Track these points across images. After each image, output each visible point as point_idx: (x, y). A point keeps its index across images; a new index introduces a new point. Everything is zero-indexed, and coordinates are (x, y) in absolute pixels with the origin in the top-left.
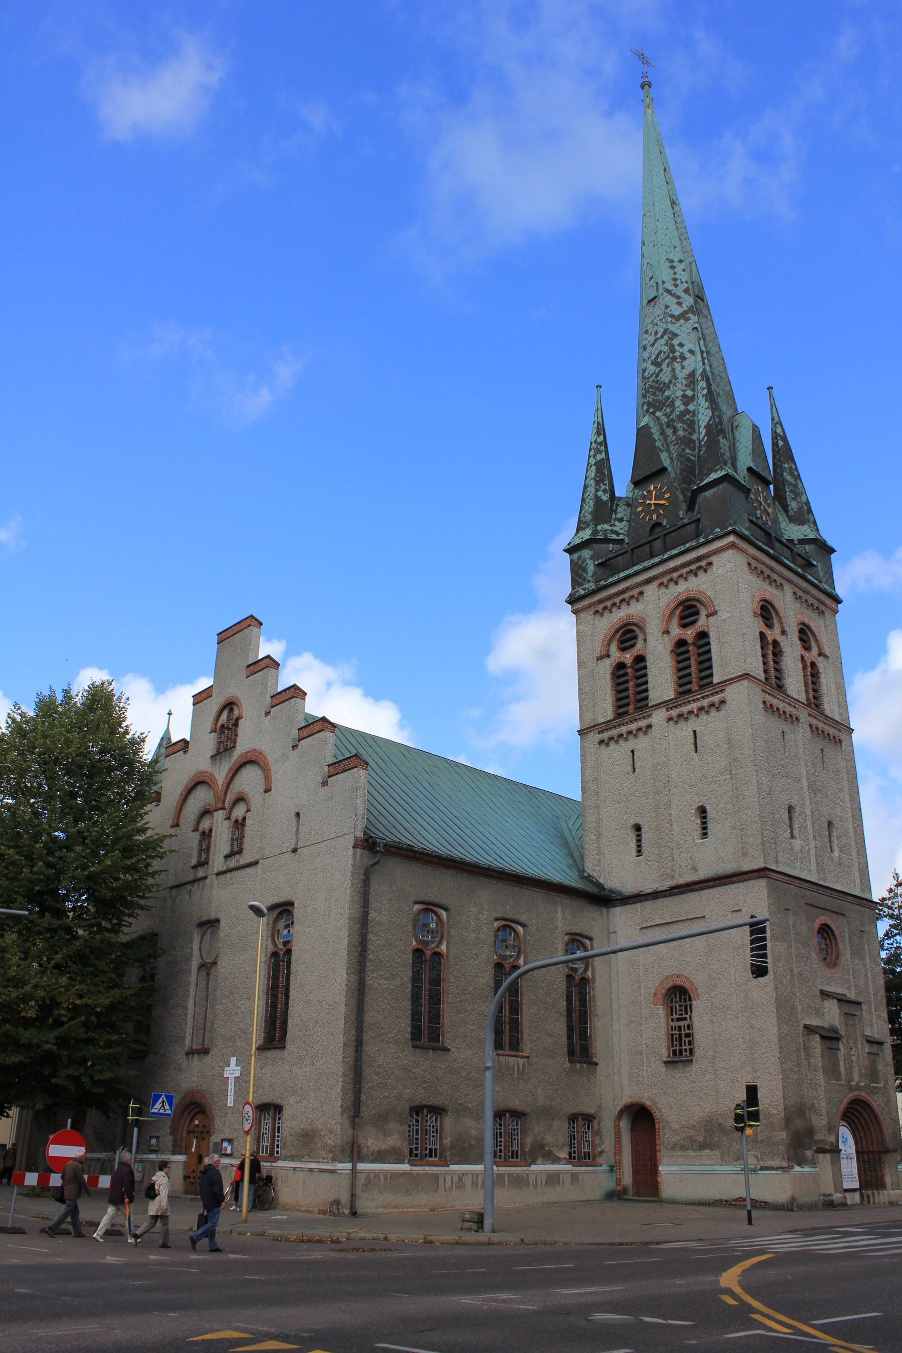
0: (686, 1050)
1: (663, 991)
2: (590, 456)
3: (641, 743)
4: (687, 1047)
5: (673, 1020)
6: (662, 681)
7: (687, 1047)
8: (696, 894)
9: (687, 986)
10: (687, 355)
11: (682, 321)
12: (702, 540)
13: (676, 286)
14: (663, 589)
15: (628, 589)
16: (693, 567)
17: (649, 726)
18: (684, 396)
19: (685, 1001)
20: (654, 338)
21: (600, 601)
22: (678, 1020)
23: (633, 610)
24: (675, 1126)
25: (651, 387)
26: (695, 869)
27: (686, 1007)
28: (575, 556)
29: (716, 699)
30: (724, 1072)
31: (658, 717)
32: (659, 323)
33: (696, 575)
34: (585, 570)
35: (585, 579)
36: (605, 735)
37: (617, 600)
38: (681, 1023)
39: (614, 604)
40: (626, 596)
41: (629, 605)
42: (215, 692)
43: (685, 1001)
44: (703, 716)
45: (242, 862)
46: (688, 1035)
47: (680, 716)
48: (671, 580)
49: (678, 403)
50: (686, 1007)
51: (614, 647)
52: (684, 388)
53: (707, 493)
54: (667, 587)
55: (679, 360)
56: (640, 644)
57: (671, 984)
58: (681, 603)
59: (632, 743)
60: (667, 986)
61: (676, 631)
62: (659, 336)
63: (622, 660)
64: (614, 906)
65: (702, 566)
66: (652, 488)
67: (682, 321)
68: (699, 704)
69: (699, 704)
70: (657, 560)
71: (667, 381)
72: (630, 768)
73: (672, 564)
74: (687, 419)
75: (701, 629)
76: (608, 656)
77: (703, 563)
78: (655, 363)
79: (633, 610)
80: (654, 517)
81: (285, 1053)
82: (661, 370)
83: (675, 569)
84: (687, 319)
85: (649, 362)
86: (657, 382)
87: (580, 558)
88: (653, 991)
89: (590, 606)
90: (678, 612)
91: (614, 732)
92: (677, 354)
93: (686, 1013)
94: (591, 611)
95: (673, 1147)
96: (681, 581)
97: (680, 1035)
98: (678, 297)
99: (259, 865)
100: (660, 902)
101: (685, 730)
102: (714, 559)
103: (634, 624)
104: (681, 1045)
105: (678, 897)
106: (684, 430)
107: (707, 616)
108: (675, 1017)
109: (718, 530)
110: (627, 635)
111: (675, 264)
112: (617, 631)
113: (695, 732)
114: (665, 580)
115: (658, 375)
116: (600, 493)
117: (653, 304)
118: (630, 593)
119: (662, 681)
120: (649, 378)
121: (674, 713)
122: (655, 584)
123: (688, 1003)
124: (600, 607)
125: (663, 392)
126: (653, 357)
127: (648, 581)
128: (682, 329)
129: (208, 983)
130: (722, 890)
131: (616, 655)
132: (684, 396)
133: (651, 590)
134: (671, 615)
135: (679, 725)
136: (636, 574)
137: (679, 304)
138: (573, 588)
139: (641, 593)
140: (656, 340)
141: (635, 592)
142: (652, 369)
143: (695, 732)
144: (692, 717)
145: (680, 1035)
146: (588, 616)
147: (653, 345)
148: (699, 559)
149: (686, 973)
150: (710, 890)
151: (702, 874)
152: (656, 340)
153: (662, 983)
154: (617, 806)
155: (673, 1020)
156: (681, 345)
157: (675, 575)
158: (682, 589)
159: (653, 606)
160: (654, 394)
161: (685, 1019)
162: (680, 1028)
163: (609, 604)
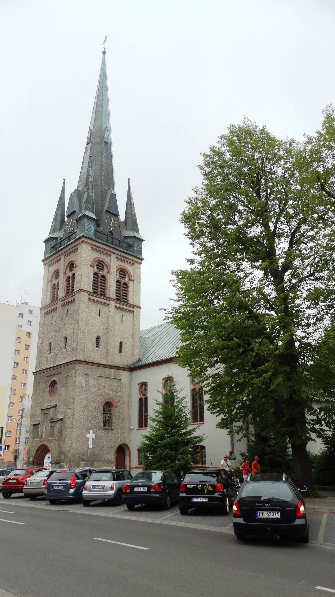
3: (104, 309)
6: (111, 290)
17: (108, 304)
21: (95, 246)
29: (131, 309)
46: (108, 420)
56: (105, 272)
79: (106, 259)
103: (106, 265)
119: (111, 290)
121: (118, 305)
124: (94, 248)
127: (114, 253)
133: (113, 257)
141: (109, 253)
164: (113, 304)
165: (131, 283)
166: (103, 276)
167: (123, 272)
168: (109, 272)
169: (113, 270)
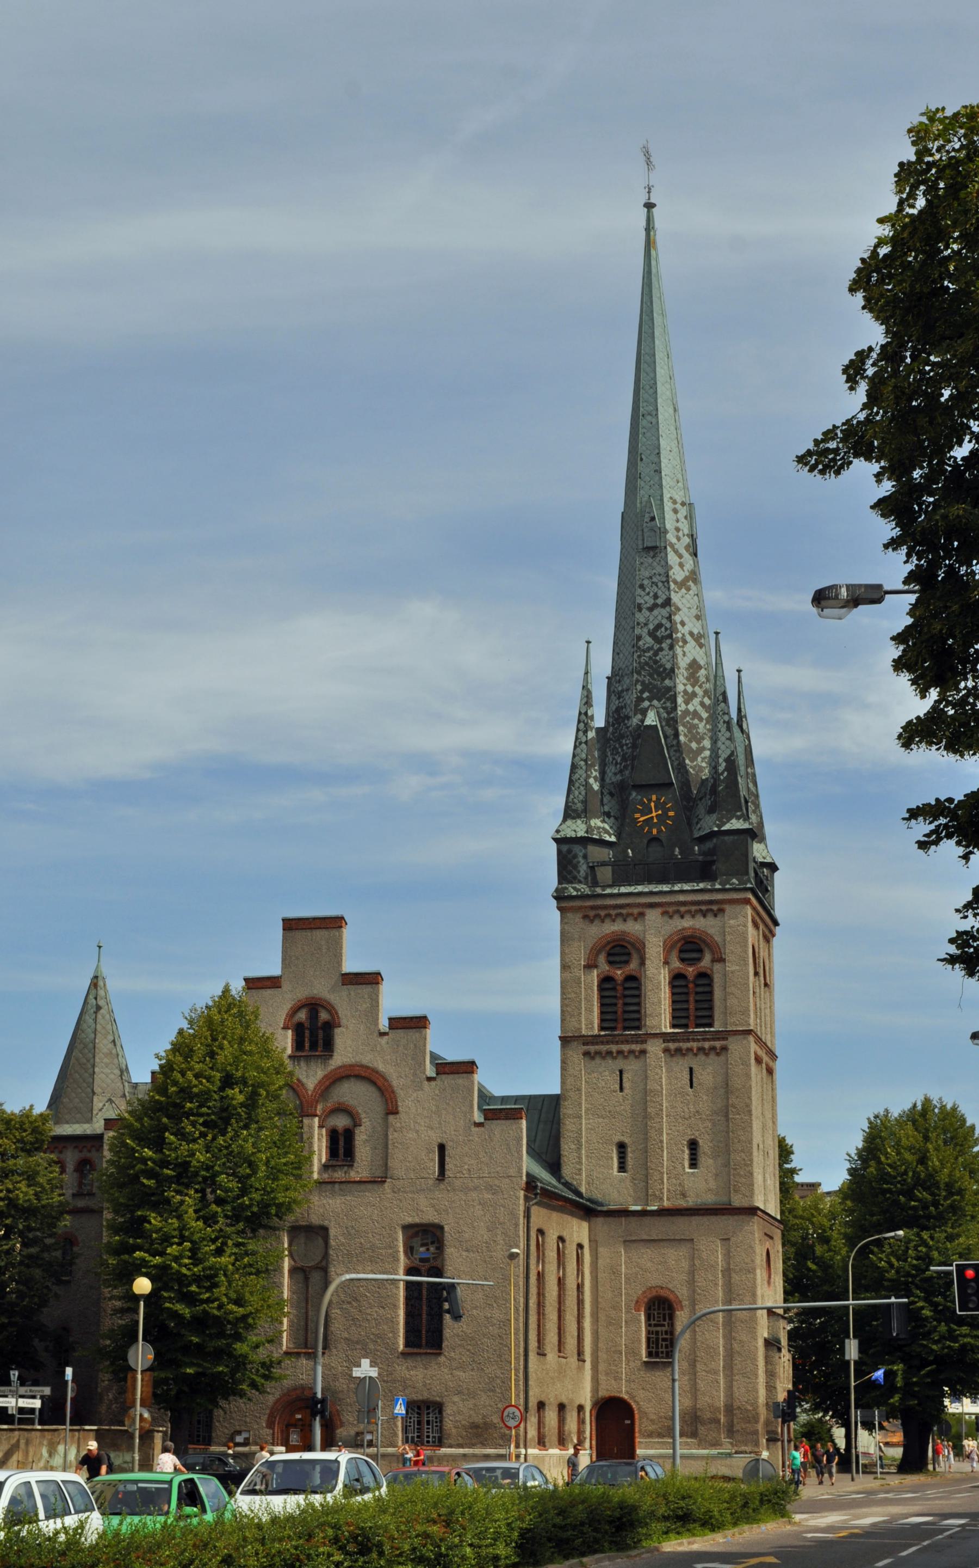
0: (662, 1352)
1: (646, 1300)
2: (578, 730)
3: (632, 1067)
4: (664, 1350)
5: (650, 1325)
7: (664, 1350)
8: (686, 1218)
9: (671, 1297)
10: (688, 638)
11: (683, 591)
12: (718, 886)
13: (679, 539)
14: (666, 918)
15: (628, 905)
16: (704, 908)
18: (685, 692)
19: (664, 1309)
20: (652, 601)
21: (592, 908)
22: (656, 1325)
23: (632, 928)
24: (654, 1417)
25: (646, 664)
26: (684, 1195)
27: (664, 1315)
28: (565, 848)
29: (718, 1044)
30: (704, 1373)
31: (655, 1048)
32: (660, 584)
33: (704, 916)
34: (576, 867)
35: (575, 878)
36: (592, 1048)
37: (613, 912)
38: (659, 1329)
39: (609, 915)
40: (624, 911)
41: (625, 920)
42: (286, 986)
43: (664, 1309)
44: (702, 1057)
45: (354, 1175)
46: (664, 1340)
47: (679, 1050)
48: (678, 912)
49: (680, 700)
50: (664, 1315)
51: (602, 959)
52: (685, 681)
53: (726, 838)
54: (671, 917)
55: (680, 644)
56: (633, 965)
57: (654, 1294)
58: (684, 938)
59: (620, 1063)
60: (649, 1296)
61: (676, 964)
62: (659, 601)
63: (611, 974)
64: (597, 1216)
65: (714, 909)
66: (654, 798)
67: (683, 591)
68: (700, 1044)
69: (700, 1044)
70: (666, 888)
71: (668, 666)
72: (618, 1087)
73: (682, 898)
74: (688, 722)
75: (703, 970)
76: (596, 967)
77: (715, 908)
78: (652, 634)
79: (632, 928)
80: (655, 831)
81: (442, 1359)
82: (661, 649)
83: (684, 904)
84: (688, 589)
85: (646, 630)
86: (656, 662)
87: (569, 851)
88: (635, 1299)
89: (580, 908)
90: (679, 945)
91: (603, 1048)
92: (679, 635)
93: (664, 1320)
94: (580, 915)
95: (650, 1435)
96: (687, 917)
97: (657, 1339)
98: (680, 556)
99: (386, 1185)
100: (647, 1220)
101: (681, 1067)
102: (727, 908)
103: (633, 945)
104: (657, 1348)
105: (666, 1218)
106: (685, 735)
107: (713, 961)
108: (653, 1322)
109: (734, 881)
110: (621, 950)
111: (678, 506)
112: (609, 943)
113: (691, 1069)
114: (671, 910)
115: (656, 654)
116: (591, 781)
117: (652, 554)
118: (630, 911)
120: (644, 651)
121: (672, 1046)
122: (660, 910)
123: (667, 1312)
124: (592, 913)
125: (663, 680)
126: (651, 627)
127: (652, 906)
128: (684, 601)
129: (307, 1287)
130: (713, 1219)
131: (604, 967)
132: (685, 692)
133: (653, 916)
134: (672, 947)
135: (675, 1059)
136: (640, 894)
137: (681, 565)
138: (560, 883)
139: (642, 915)
140: (655, 606)
141: (636, 911)
142: (649, 640)
143: (691, 1069)
144: (690, 1055)
145: (657, 1339)
146: (577, 918)
147: (651, 609)
148: (711, 902)
149: (670, 1286)
150: (700, 1217)
151: (690, 1202)
152: (655, 606)
153: (644, 1292)
154: (600, 1120)
155: (650, 1325)
156: (683, 624)
157: (683, 909)
158: (687, 923)
159: (655, 933)
160: (651, 675)
161: (664, 1325)
162: (657, 1333)
163: (602, 913)
164: (655, 1048)
165: (717, 967)
166: (631, 978)
167: (690, 947)
168: (642, 963)
169: (654, 949)
